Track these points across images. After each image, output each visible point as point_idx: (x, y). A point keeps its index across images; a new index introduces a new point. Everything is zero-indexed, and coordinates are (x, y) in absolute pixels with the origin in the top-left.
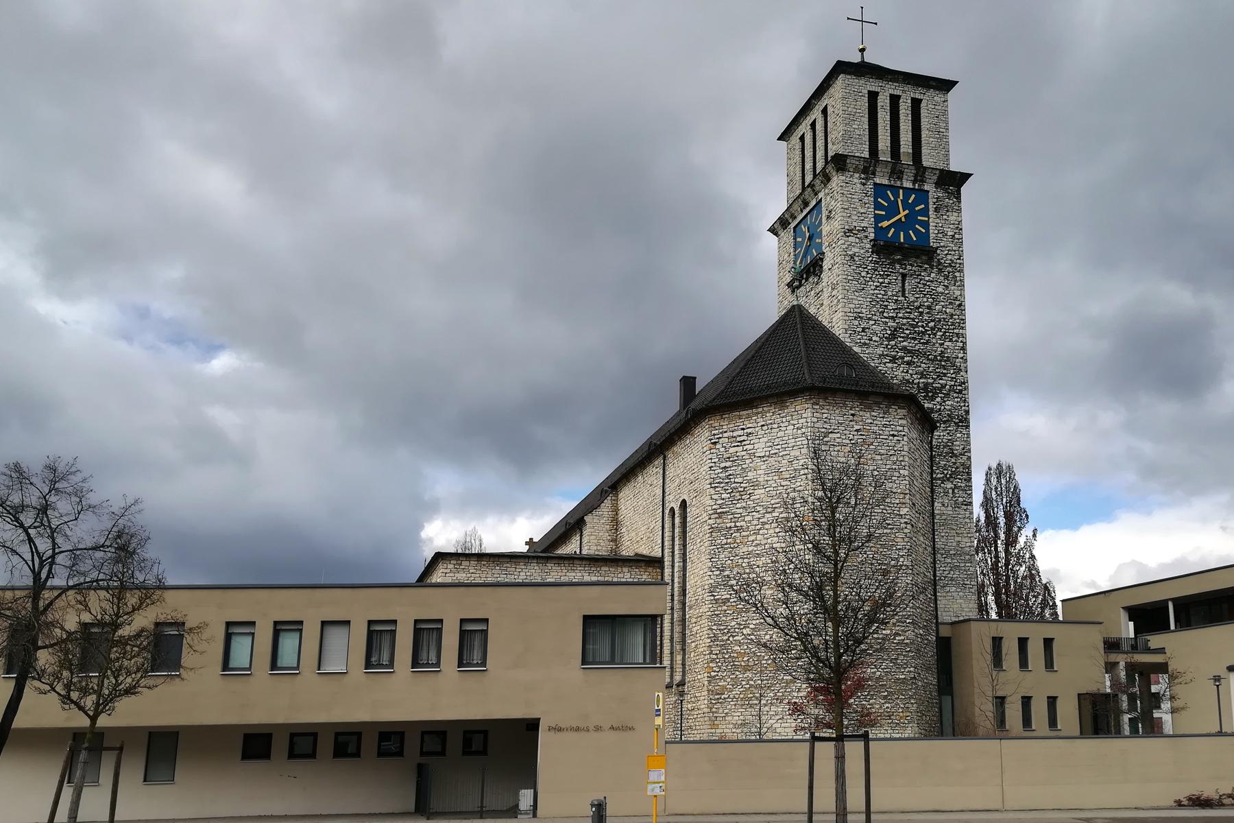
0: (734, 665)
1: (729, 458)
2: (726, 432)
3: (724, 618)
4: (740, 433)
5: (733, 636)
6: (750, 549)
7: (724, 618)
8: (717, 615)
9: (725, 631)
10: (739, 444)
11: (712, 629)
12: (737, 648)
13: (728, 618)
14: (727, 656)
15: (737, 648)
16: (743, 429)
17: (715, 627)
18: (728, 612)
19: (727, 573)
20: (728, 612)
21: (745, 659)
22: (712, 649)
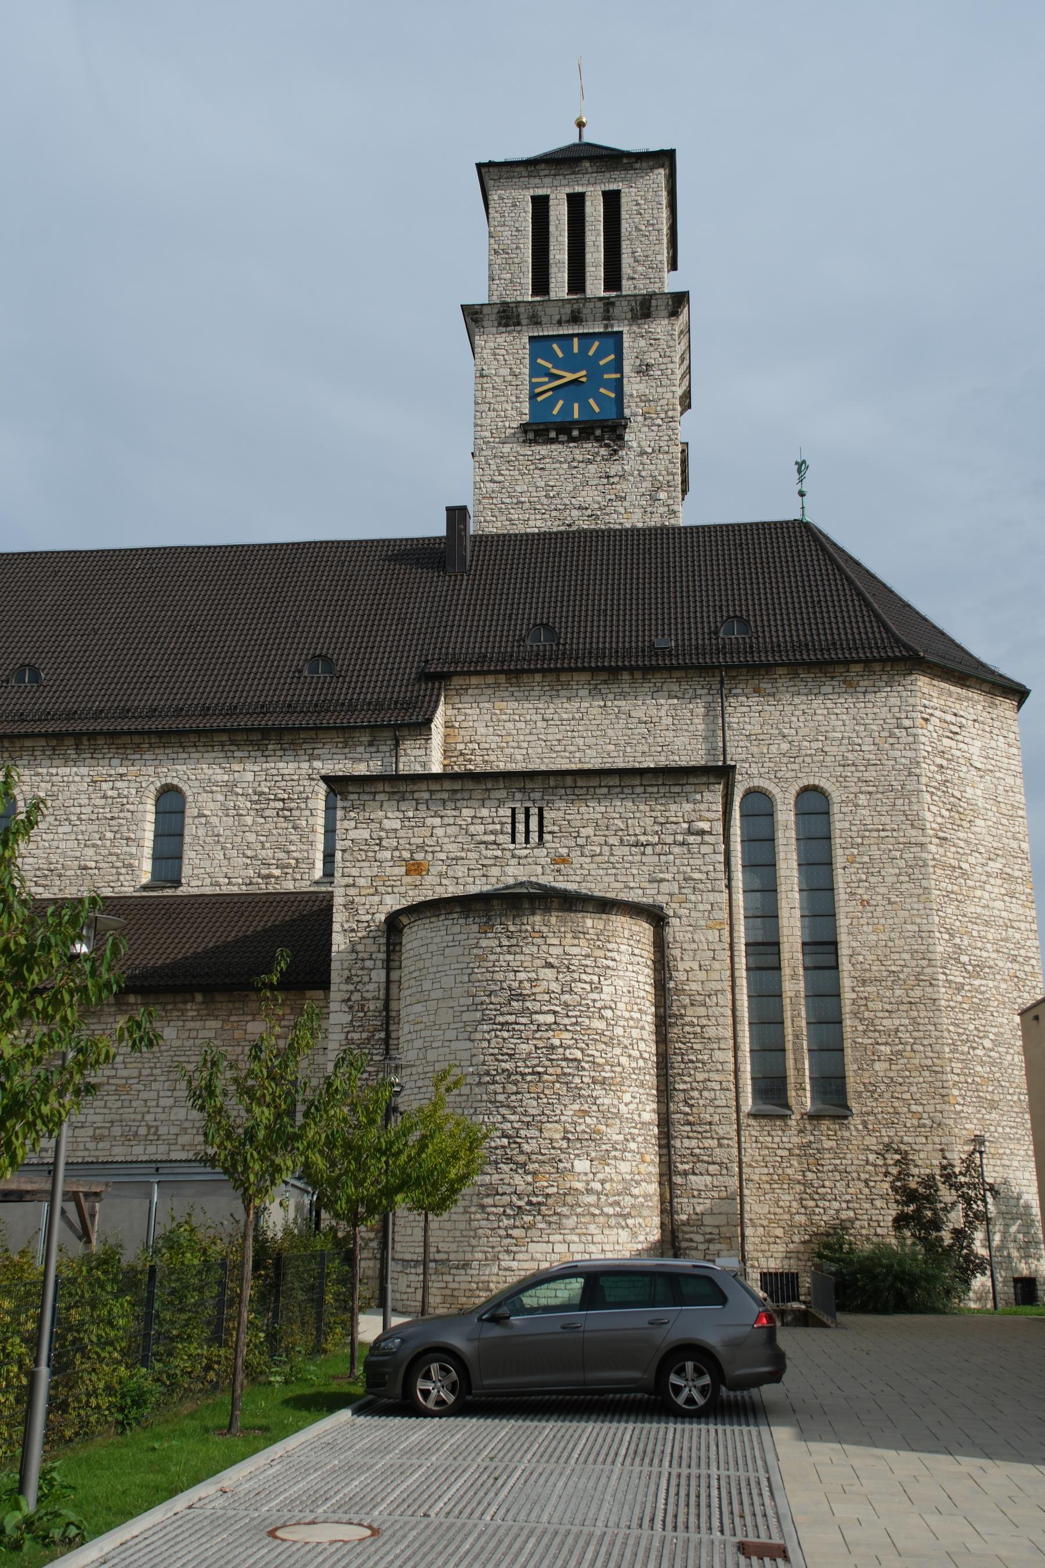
0: (979, 1097)
1: (943, 752)
2: (936, 709)
3: (960, 1015)
4: (953, 719)
5: (974, 1048)
6: (979, 910)
7: (960, 1015)
8: (953, 1008)
9: (964, 1037)
10: (951, 735)
11: (949, 1031)
12: (979, 1068)
13: (967, 1016)
14: (970, 1081)
15: (979, 1068)
16: (955, 715)
17: (951, 1028)
18: (964, 1006)
19: (957, 941)
20: (964, 1006)
21: (990, 1089)
22: (953, 1065)
